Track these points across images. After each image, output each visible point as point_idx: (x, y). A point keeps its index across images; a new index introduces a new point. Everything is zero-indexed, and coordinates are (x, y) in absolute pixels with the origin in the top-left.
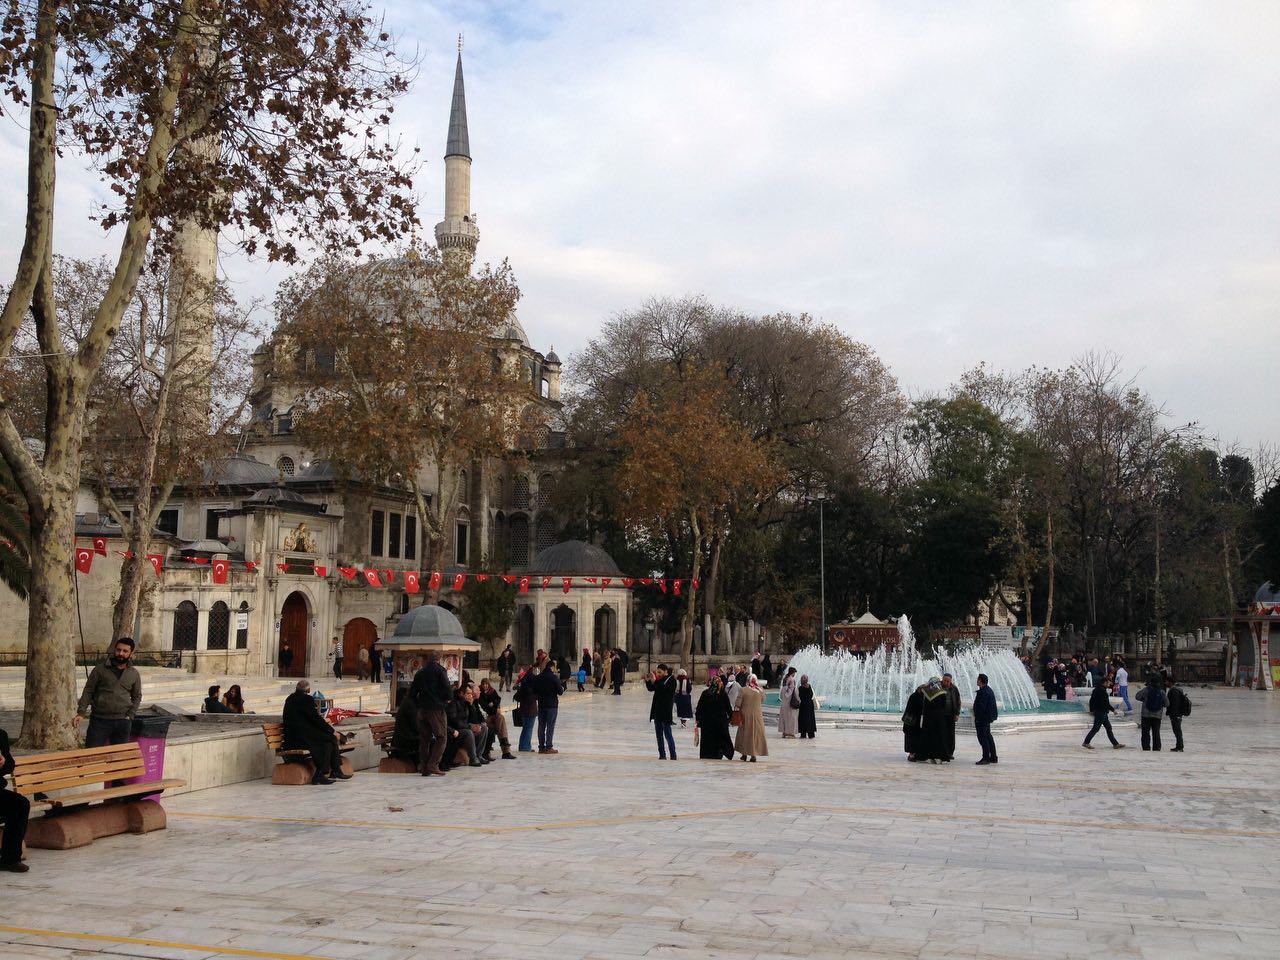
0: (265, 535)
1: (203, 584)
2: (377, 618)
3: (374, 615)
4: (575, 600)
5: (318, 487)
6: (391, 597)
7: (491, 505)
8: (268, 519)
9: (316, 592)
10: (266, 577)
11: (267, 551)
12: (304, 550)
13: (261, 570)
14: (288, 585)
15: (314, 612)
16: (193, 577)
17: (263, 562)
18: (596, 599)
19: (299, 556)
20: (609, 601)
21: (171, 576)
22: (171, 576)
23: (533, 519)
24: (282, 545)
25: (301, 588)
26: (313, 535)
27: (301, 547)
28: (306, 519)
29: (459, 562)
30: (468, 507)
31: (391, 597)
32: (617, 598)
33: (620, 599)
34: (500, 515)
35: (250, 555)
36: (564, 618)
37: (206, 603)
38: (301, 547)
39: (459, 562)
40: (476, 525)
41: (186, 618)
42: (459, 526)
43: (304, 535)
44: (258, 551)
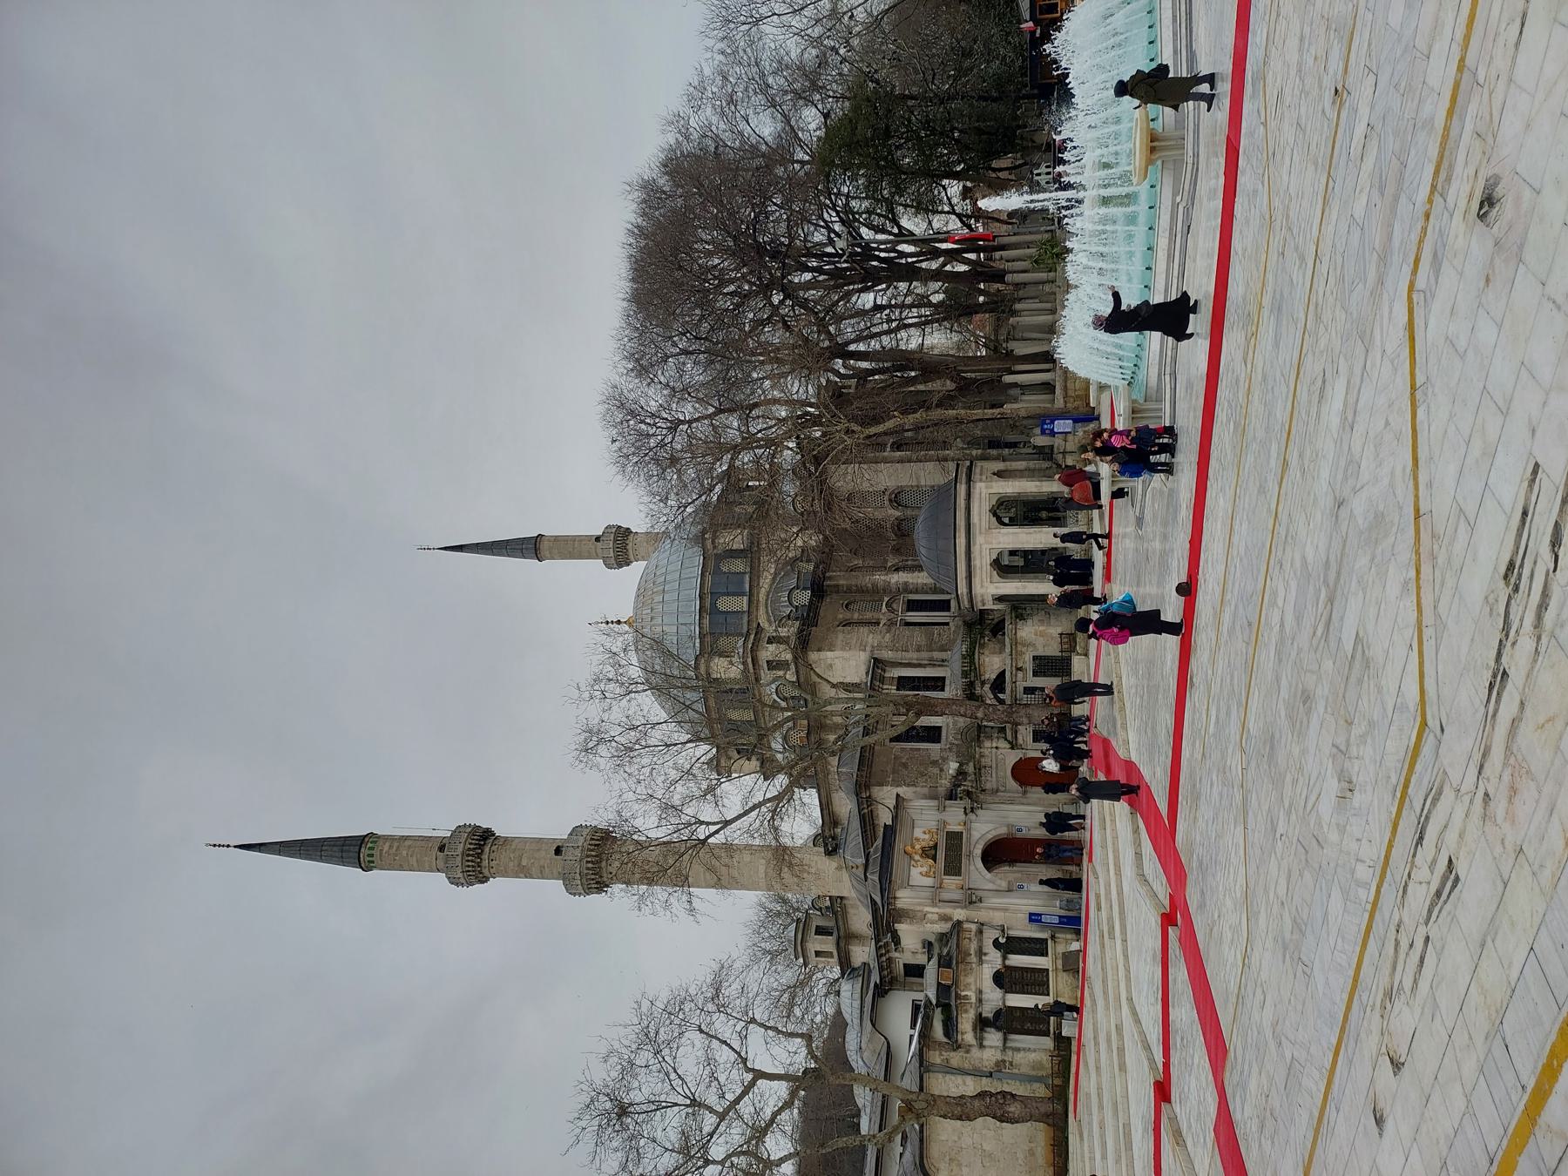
0: (918, 908)
1: (973, 1000)
2: (1012, 757)
3: (1007, 762)
4: (986, 553)
5: (866, 811)
6: (987, 744)
7: (883, 568)
8: (900, 904)
9: (985, 828)
10: (965, 907)
11: (933, 906)
12: (935, 847)
13: (959, 914)
14: (976, 872)
15: (1003, 831)
16: (966, 1011)
17: (947, 910)
18: (985, 524)
19: (941, 855)
20: (986, 507)
21: (965, 1037)
22: (965, 1037)
23: (897, 514)
24: (929, 881)
25: (978, 851)
26: (918, 833)
27: (930, 852)
28: (899, 846)
29: (948, 609)
30: (886, 599)
31: (987, 744)
32: (983, 495)
33: (984, 491)
34: (897, 550)
35: (944, 927)
36: (1003, 567)
37: (994, 998)
38: (930, 852)
39: (948, 609)
40: (906, 588)
41: (1008, 1021)
42: (908, 610)
43: (918, 847)
44: (936, 917)
